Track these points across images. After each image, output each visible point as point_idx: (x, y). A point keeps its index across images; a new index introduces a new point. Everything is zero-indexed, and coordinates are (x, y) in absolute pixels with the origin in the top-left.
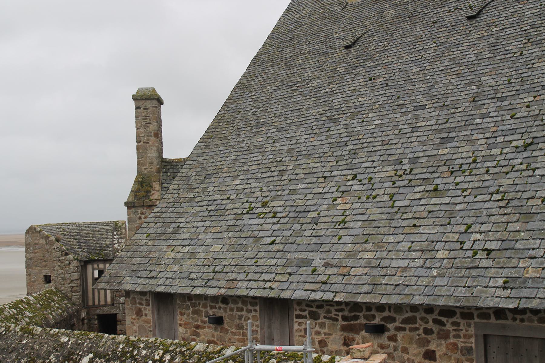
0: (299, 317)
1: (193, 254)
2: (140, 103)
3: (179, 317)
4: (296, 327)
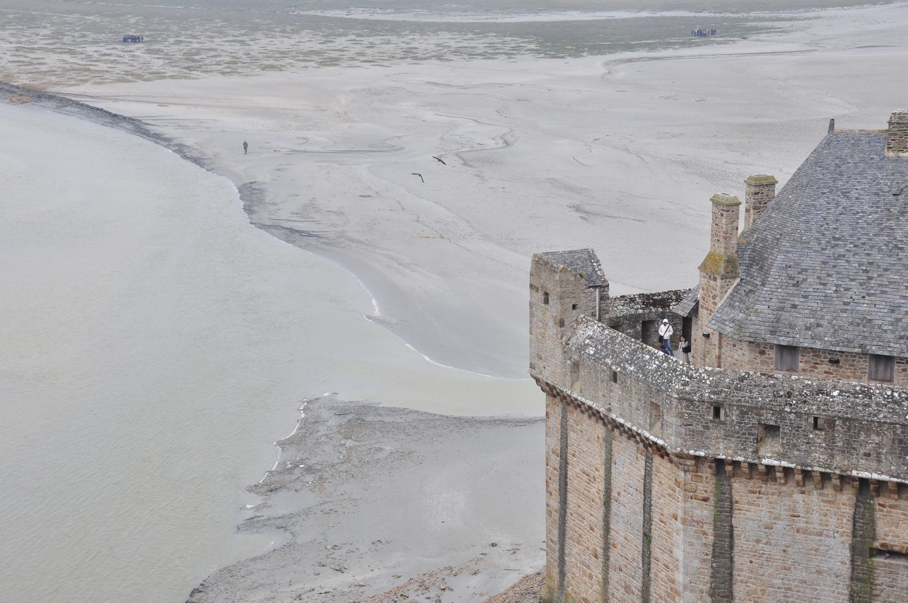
0: (897, 363)
1: (819, 325)
2: (729, 208)
3: (800, 357)
4: (896, 367)
